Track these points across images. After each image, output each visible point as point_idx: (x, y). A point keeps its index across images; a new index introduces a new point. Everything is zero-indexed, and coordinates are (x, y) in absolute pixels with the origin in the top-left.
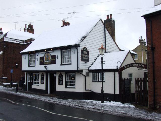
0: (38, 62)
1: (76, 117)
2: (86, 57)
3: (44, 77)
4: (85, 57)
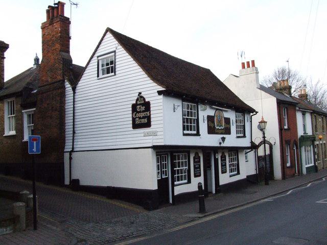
0: (203, 127)
1: (183, 229)
2: (144, 118)
3: (199, 162)
4: (140, 118)
